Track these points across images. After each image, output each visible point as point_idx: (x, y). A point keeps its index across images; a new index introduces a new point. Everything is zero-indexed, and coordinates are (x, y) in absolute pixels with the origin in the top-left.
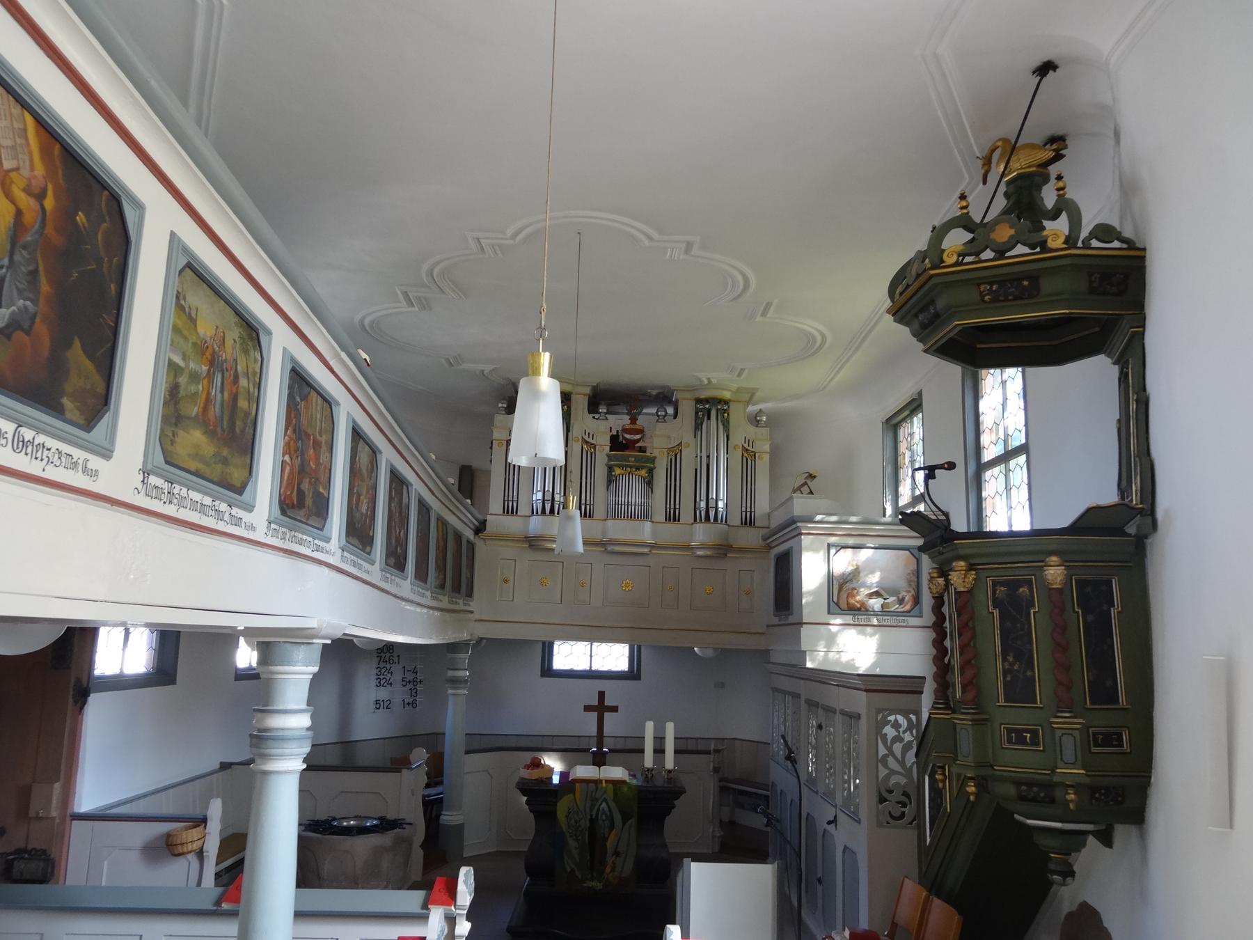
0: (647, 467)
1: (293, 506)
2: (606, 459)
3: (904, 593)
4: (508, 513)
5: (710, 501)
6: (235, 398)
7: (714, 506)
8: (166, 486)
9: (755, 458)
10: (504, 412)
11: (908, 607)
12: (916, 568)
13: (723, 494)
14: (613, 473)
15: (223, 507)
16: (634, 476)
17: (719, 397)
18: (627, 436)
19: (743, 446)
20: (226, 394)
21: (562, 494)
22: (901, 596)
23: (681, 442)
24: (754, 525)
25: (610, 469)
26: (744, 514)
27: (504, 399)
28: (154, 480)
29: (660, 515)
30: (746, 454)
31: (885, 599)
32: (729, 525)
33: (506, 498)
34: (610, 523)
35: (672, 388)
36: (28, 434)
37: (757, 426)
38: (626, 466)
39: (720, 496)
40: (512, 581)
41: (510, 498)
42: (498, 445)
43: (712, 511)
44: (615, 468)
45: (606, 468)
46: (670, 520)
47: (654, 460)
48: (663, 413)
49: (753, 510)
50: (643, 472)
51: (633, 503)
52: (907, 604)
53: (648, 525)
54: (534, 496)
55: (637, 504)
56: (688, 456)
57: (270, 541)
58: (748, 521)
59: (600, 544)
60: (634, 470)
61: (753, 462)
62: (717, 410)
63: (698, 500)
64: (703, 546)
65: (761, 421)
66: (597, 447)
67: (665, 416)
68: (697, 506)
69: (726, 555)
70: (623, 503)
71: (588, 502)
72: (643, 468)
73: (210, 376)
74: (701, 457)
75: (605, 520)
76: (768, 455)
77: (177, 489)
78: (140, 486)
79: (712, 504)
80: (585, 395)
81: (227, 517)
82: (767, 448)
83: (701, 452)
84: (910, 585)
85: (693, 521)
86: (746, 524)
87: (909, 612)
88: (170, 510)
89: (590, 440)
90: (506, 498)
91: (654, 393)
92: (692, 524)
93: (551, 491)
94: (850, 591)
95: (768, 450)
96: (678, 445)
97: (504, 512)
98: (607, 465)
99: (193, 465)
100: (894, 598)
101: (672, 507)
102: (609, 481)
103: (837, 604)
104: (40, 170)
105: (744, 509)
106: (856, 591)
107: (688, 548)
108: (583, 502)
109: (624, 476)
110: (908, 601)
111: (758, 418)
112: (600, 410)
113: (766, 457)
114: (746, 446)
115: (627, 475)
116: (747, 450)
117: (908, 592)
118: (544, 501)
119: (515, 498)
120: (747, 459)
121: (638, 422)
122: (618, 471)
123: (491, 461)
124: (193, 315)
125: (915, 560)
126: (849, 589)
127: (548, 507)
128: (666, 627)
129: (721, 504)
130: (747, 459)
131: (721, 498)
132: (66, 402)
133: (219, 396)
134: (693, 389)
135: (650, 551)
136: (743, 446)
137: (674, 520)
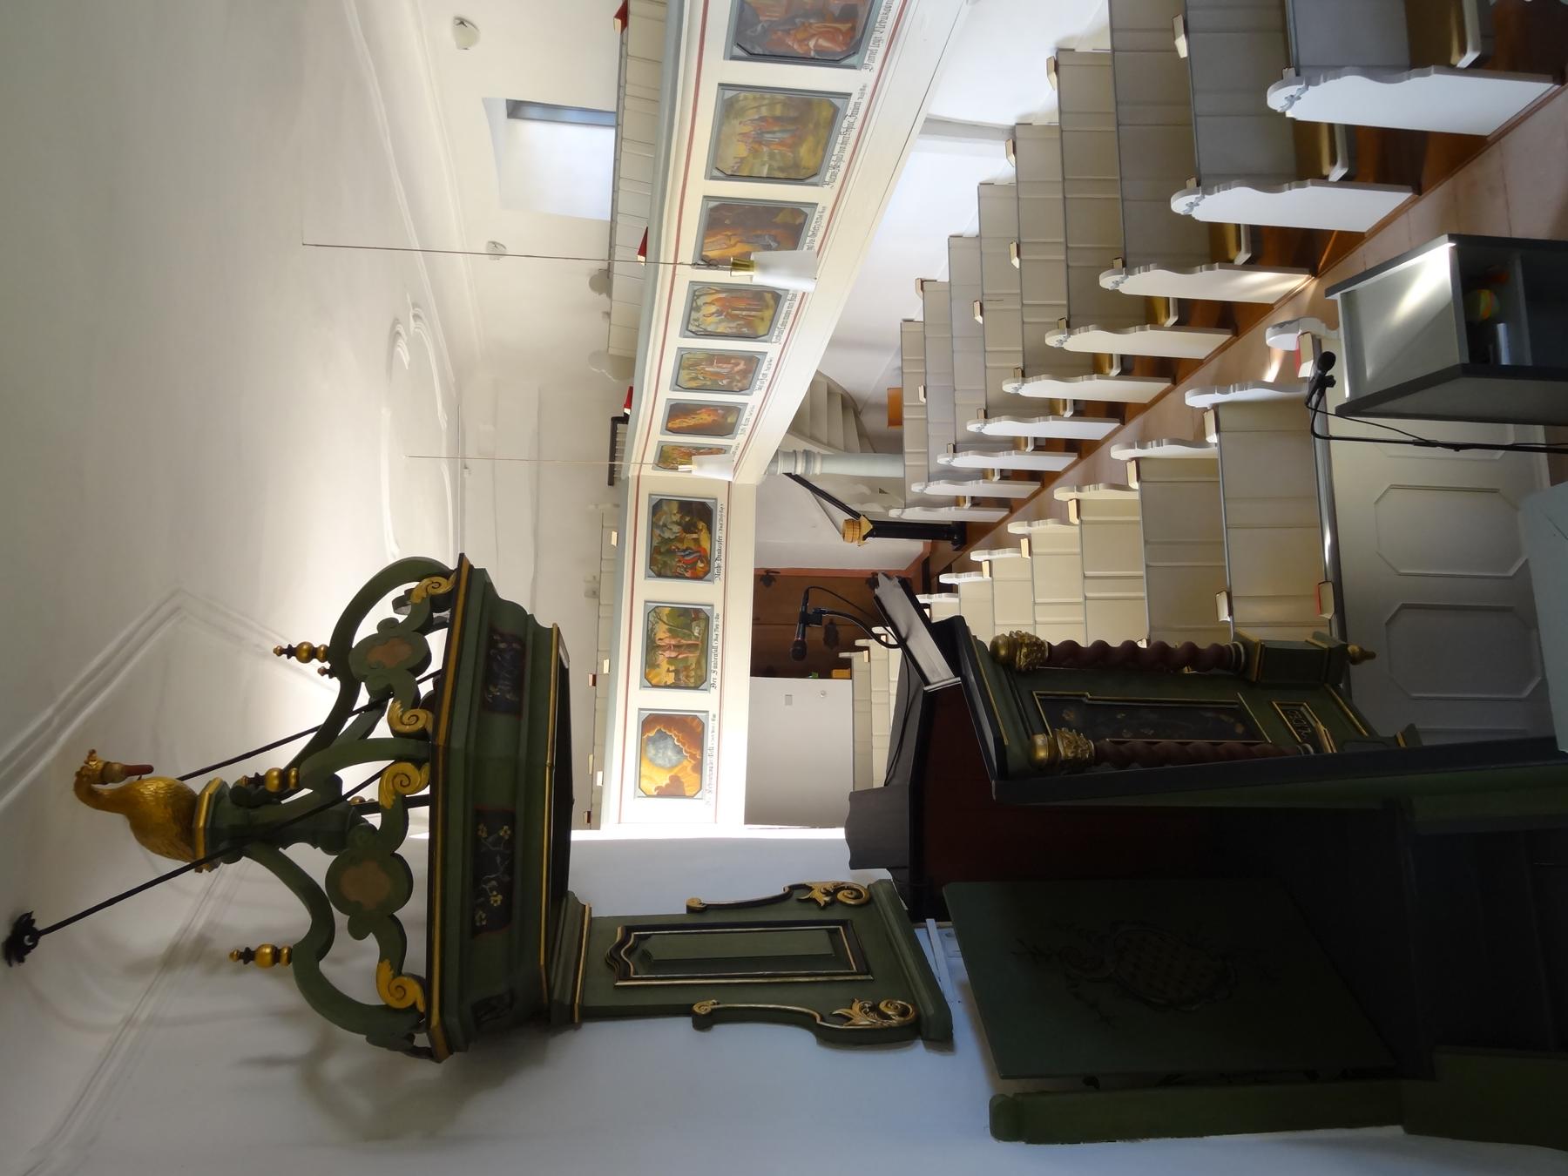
1: (853, 29)
6: (777, 119)
8: (831, 171)
15: (845, 124)
20: (776, 129)
28: (827, 179)
36: (810, 233)
57: (877, 65)
73: (768, 144)
77: (832, 163)
78: (830, 186)
81: (852, 120)
88: (843, 166)
99: (820, 153)
104: (719, 237)
124: (739, 160)
132: (798, 222)
133: (779, 135)
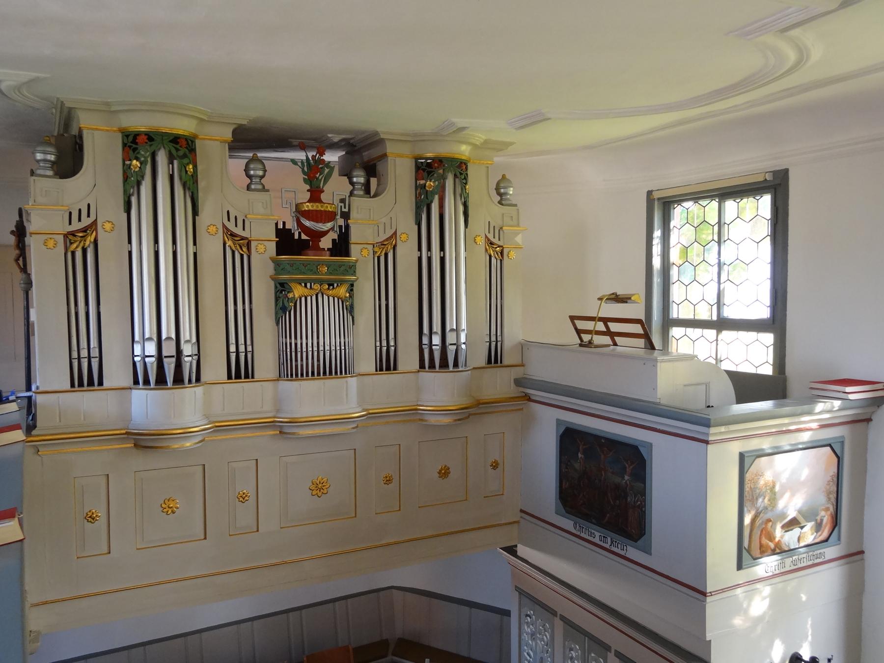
2: (270, 269)
3: (823, 513)
4: (81, 384)
10: (50, 173)
11: (825, 534)
12: (836, 470)
14: (291, 295)
16: (326, 298)
22: (819, 518)
23: (395, 233)
24: (501, 362)
25: (282, 288)
29: (366, 362)
31: (802, 528)
33: (75, 355)
34: (289, 387)
35: (382, 136)
38: (312, 281)
39: (461, 324)
40: (102, 514)
41: (84, 353)
44: (293, 285)
45: (272, 283)
49: (499, 339)
50: (342, 291)
52: (825, 526)
53: (353, 382)
56: (407, 253)
58: (494, 358)
59: (272, 424)
62: (455, 176)
65: (506, 194)
66: (253, 244)
72: (341, 282)
74: (443, 260)
75: (278, 380)
80: (224, 142)
84: (829, 499)
87: (826, 540)
89: (238, 231)
90: (75, 355)
91: (336, 138)
94: (764, 526)
96: (391, 237)
97: (73, 385)
98: (272, 278)
100: (813, 523)
103: (749, 551)
106: (771, 523)
109: (309, 299)
110: (826, 524)
111: (502, 191)
114: (491, 236)
115: (314, 298)
117: (827, 509)
119: (95, 353)
121: (323, 197)
125: (836, 460)
126: (762, 524)
127: (170, 366)
128: (384, 542)
134: (416, 138)
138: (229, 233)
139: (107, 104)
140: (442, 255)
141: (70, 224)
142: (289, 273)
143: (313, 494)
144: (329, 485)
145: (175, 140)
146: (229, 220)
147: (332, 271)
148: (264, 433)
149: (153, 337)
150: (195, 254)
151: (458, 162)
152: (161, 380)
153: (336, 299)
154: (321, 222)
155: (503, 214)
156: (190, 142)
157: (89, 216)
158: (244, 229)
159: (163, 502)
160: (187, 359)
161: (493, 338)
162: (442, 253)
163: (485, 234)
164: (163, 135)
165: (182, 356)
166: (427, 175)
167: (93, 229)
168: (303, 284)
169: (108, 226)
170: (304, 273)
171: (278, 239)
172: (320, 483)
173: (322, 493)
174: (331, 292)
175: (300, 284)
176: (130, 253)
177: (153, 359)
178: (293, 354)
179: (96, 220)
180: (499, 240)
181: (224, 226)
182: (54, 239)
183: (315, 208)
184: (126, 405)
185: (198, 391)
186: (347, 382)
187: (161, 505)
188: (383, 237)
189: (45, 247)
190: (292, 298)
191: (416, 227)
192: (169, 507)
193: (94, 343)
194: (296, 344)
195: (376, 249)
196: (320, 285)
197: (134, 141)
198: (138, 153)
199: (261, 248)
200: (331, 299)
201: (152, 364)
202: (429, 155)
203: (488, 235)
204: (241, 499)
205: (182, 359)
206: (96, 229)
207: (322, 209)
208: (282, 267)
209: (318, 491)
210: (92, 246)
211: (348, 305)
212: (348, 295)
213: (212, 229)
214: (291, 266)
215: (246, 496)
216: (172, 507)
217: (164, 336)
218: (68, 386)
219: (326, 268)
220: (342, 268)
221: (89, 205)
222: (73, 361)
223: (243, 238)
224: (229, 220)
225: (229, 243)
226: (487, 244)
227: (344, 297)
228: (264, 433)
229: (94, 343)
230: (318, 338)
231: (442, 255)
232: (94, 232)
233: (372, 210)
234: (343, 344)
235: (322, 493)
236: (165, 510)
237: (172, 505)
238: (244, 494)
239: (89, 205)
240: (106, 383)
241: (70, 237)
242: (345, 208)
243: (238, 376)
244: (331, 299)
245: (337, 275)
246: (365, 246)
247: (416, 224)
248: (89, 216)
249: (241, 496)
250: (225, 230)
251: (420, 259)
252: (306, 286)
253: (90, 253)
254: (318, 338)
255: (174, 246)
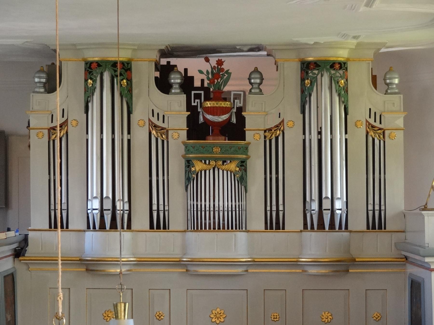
0: (237, 159)
5: (324, 201)
7: (330, 208)
9: (384, 137)
13: (340, 191)
14: (193, 169)
16: (221, 172)
17: (332, 59)
18: (209, 117)
19: (367, 121)
21: (126, 199)
23: (283, 121)
24: (385, 228)
25: (189, 163)
26: (371, 213)
27: (41, 71)
30: (371, 133)
32: (350, 232)
33: (52, 207)
34: (192, 236)
37: (386, 93)
38: (210, 159)
39: (336, 193)
41: (58, 207)
42: (37, 135)
43: (328, 214)
44: (195, 162)
45: (183, 162)
46: (271, 228)
47: (247, 148)
48: (258, 81)
49: (383, 208)
50: (233, 166)
51: (221, 208)
53: (241, 236)
54: (89, 203)
55: (226, 209)
59: (178, 263)
60: (221, 163)
61: (382, 142)
63: (308, 199)
64: (316, 263)
65: (391, 84)
67: (260, 84)
68: (307, 207)
69: (348, 271)
70: (207, 209)
71: (161, 208)
72: (232, 160)
74: (310, 140)
75: (185, 231)
76: (402, 132)
79: (326, 204)
82: (400, 123)
83: (310, 133)
85: (302, 229)
86: (374, 228)
89: (160, 123)
90: (52, 207)
92: (301, 231)
93: (110, 196)
95: (402, 126)
96: (280, 124)
98: (184, 157)
101: (274, 208)
102: (188, 180)
105: (370, 207)
107: (295, 264)
108: (155, 207)
109: (207, 172)
111: (388, 81)
112: (172, 81)
113: (400, 136)
114: (372, 121)
115: (212, 171)
116: (373, 127)
118: (102, 210)
119: (64, 207)
120: (373, 140)
122: (198, 166)
123: (29, 146)
129: (338, 205)
130: (373, 140)
131: (339, 196)
135: (247, 271)
136: (367, 121)
137: (278, 228)
138: (153, 125)
139: (74, 45)
140: (319, 138)
141: (52, 122)
142: (192, 153)
143: (213, 321)
144: (225, 316)
145: (114, 64)
146: (153, 116)
147: (225, 151)
148: (175, 270)
149: (98, 197)
150: (129, 141)
151: (330, 63)
152: (102, 227)
153: (229, 173)
154: (217, 115)
155: (385, 101)
156: (126, 65)
157: (63, 117)
158: (164, 122)
159: (104, 312)
160: (118, 212)
161: (377, 207)
162: (319, 136)
163: (366, 119)
164: (107, 62)
165: (116, 210)
166: (306, 75)
167: (65, 125)
168: (203, 161)
169: (74, 123)
170: (203, 153)
171: (188, 129)
172: (218, 313)
173: (220, 321)
174: (224, 167)
175: (201, 161)
176: (87, 140)
177: (97, 211)
178: (195, 212)
179: (67, 119)
180: (381, 123)
181: (150, 120)
182: (42, 132)
183: (212, 105)
184: (81, 241)
185: (127, 235)
186: (235, 235)
187: (103, 314)
188: (271, 124)
189: (37, 138)
190: (194, 171)
191: (302, 116)
192: (108, 316)
193: (64, 200)
194: (197, 205)
195: (267, 134)
196: (216, 162)
197: (90, 68)
198: (92, 74)
199: (176, 135)
200: (225, 172)
201: (97, 214)
202: (311, 59)
203: (369, 120)
204: (158, 317)
205: (116, 212)
206: (67, 125)
207: (217, 106)
208: (188, 149)
209: (217, 319)
210: (65, 136)
211: (238, 177)
212: (238, 169)
213: (141, 123)
214: (193, 148)
215: (162, 316)
216: (110, 316)
217: (105, 195)
218: (47, 227)
219: (220, 149)
220: (233, 149)
221: (63, 110)
222: (51, 211)
223: (163, 129)
224: (153, 116)
225: (154, 132)
226: (367, 127)
227: (234, 171)
228: (175, 270)
229: (64, 200)
230: (214, 201)
231: (319, 138)
232: (66, 127)
233: (263, 105)
234: (234, 206)
235: (220, 321)
236: (105, 318)
237: (110, 315)
238: (160, 314)
239: (63, 110)
240: (70, 227)
241: (52, 131)
242: (240, 103)
243: (158, 227)
244: (225, 172)
245: (229, 154)
246: (257, 132)
247: (301, 114)
248: (63, 117)
249: (158, 315)
250: (151, 123)
251: (304, 141)
252: (205, 163)
253: (64, 141)
254: (214, 201)
255: (113, 135)
